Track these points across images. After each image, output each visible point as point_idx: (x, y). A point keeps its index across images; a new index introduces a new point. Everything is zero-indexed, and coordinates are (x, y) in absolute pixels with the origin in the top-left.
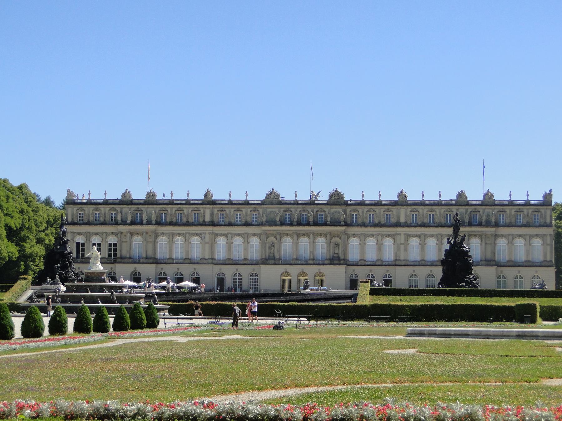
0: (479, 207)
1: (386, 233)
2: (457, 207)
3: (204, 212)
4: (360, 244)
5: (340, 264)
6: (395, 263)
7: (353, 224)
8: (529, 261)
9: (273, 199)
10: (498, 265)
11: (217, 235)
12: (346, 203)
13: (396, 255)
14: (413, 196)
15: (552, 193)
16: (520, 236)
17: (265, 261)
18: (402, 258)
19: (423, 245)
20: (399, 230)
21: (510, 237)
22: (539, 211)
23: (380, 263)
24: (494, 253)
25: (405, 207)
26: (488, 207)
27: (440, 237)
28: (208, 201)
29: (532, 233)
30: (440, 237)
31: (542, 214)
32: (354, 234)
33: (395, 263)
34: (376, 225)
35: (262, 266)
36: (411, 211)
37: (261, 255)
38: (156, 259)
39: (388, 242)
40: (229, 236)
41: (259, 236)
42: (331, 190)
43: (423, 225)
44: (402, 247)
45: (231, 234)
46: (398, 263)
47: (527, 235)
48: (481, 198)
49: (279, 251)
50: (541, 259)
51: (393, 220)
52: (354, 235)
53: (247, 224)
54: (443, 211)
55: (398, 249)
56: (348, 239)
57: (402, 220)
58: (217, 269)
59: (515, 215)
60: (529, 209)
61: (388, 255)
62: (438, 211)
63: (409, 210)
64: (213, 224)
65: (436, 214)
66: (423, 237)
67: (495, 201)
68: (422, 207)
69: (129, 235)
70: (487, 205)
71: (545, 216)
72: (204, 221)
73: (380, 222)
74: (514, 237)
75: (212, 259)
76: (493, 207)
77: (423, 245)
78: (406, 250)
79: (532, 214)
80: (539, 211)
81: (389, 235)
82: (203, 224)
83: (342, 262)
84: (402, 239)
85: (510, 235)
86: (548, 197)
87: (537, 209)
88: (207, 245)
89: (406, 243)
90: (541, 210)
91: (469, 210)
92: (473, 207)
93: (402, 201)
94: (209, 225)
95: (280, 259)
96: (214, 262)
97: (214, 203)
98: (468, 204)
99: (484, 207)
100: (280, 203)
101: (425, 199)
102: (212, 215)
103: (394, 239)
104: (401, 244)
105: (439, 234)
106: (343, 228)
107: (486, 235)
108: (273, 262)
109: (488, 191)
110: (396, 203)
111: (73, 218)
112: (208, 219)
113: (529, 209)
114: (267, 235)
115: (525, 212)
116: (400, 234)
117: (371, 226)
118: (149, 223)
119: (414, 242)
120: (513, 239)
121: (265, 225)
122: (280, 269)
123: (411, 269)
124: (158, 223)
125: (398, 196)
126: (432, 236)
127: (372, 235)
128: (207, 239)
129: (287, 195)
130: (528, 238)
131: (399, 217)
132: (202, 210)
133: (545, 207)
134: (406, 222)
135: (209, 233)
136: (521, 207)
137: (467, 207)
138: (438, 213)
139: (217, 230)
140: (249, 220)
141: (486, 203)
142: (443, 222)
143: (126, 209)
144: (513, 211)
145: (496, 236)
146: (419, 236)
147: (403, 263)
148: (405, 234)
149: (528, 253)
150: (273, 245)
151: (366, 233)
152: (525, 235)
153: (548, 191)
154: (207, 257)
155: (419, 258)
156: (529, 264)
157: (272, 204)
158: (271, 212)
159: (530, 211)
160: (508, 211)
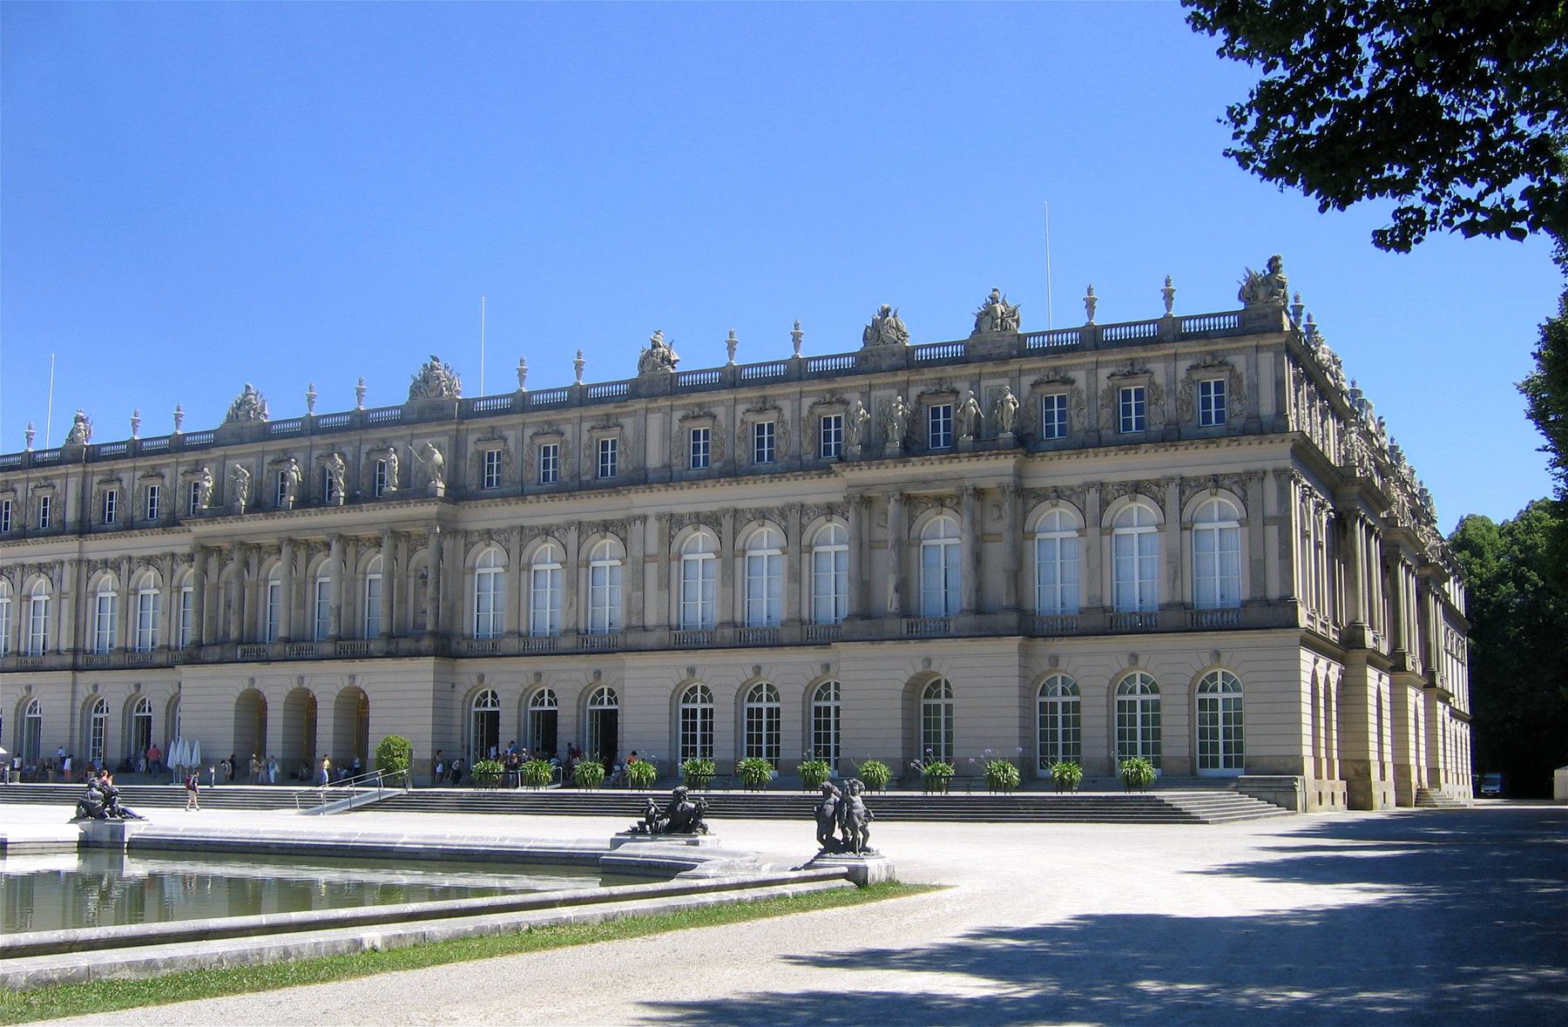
0: (950, 371)
1: (597, 518)
2: (861, 381)
4: (507, 567)
7: (487, 491)
8: (1184, 606)
10: (1030, 626)
11: (92, 566)
12: (468, 411)
13: (635, 607)
14: (695, 355)
15: (1283, 275)
16: (1136, 489)
18: (651, 620)
19: (732, 558)
21: (1092, 497)
22: (1223, 364)
24: (1017, 575)
25: (663, 402)
26: (989, 368)
27: (794, 518)
29: (1189, 472)
30: (794, 518)
31: (1235, 377)
32: (489, 532)
35: (186, 671)
36: (684, 419)
39: (606, 554)
40: (125, 566)
44: (652, 570)
45: (130, 559)
47: (1170, 480)
48: (965, 331)
50: (1240, 589)
52: (488, 535)
56: (467, 552)
57: (654, 460)
59: (1112, 390)
60: (1176, 356)
61: (609, 606)
62: (786, 406)
64: (83, 529)
65: (781, 421)
66: (727, 523)
67: (1022, 338)
68: (725, 395)
70: (986, 359)
71: (1255, 387)
72: (63, 522)
74: (1106, 493)
76: (1013, 366)
77: (732, 558)
79: (1189, 381)
80: (1223, 364)
81: (606, 527)
82: (59, 531)
83: (426, 643)
85: (1088, 486)
87: (1213, 354)
89: (670, 556)
90: (1229, 359)
91: (914, 392)
92: (930, 374)
93: (657, 382)
94: (72, 533)
96: (80, 661)
98: (909, 361)
99: (971, 369)
103: (624, 541)
105: (790, 507)
107: (979, 493)
108: (216, 652)
109: (994, 300)
110: (635, 390)
112: (71, 515)
113: (1176, 356)
115: (1159, 372)
116: (644, 518)
119: (700, 545)
120: (1104, 504)
123: (746, 659)
126: (763, 515)
127: (547, 532)
130: (1172, 492)
132: (58, 482)
133: (1250, 342)
134: (668, 466)
135: (71, 562)
136: (1139, 353)
137: (902, 377)
138: (787, 415)
139: (99, 547)
141: (982, 351)
144: (1104, 373)
145: (1024, 495)
146: (712, 520)
148: (659, 517)
149: (1176, 565)
151: (527, 522)
152: (1157, 483)
153: (1260, 268)
154: (64, 646)
155: (716, 615)
156: (1186, 618)
159: (1183, 365)
160: (1080, 377)
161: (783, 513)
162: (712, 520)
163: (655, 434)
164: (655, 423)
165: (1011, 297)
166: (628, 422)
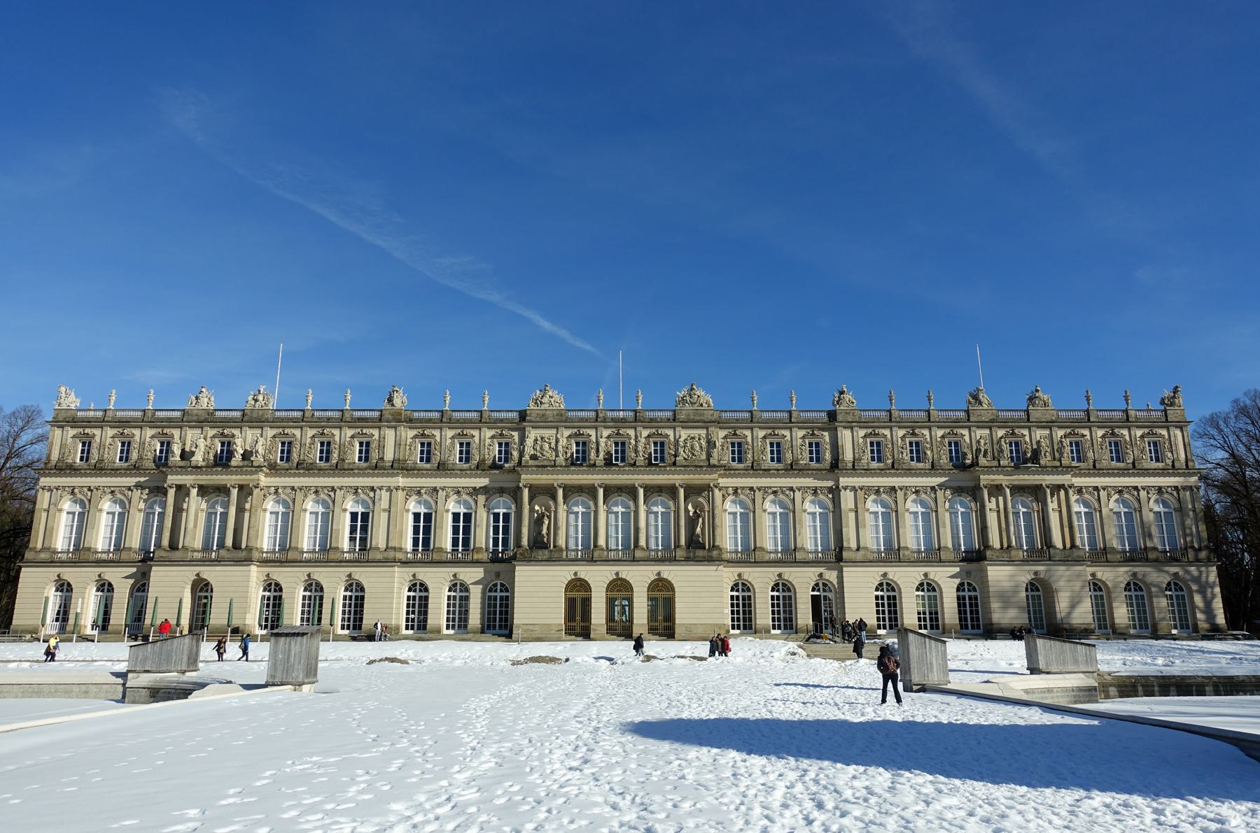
3: (382, 440)
20: (844, 481)
57: (848, 455)
64: (400, 466)
66: (900, 494)
82: (378, 468)
83: (715, 553)
96: (399, 556)
102: (397, 445)
104: (851, 510)
111: (62, 454)
112: (389, 455)
116: (845, 488)
122: (564, 574)
143: (191, 434)
147: (859, 556)
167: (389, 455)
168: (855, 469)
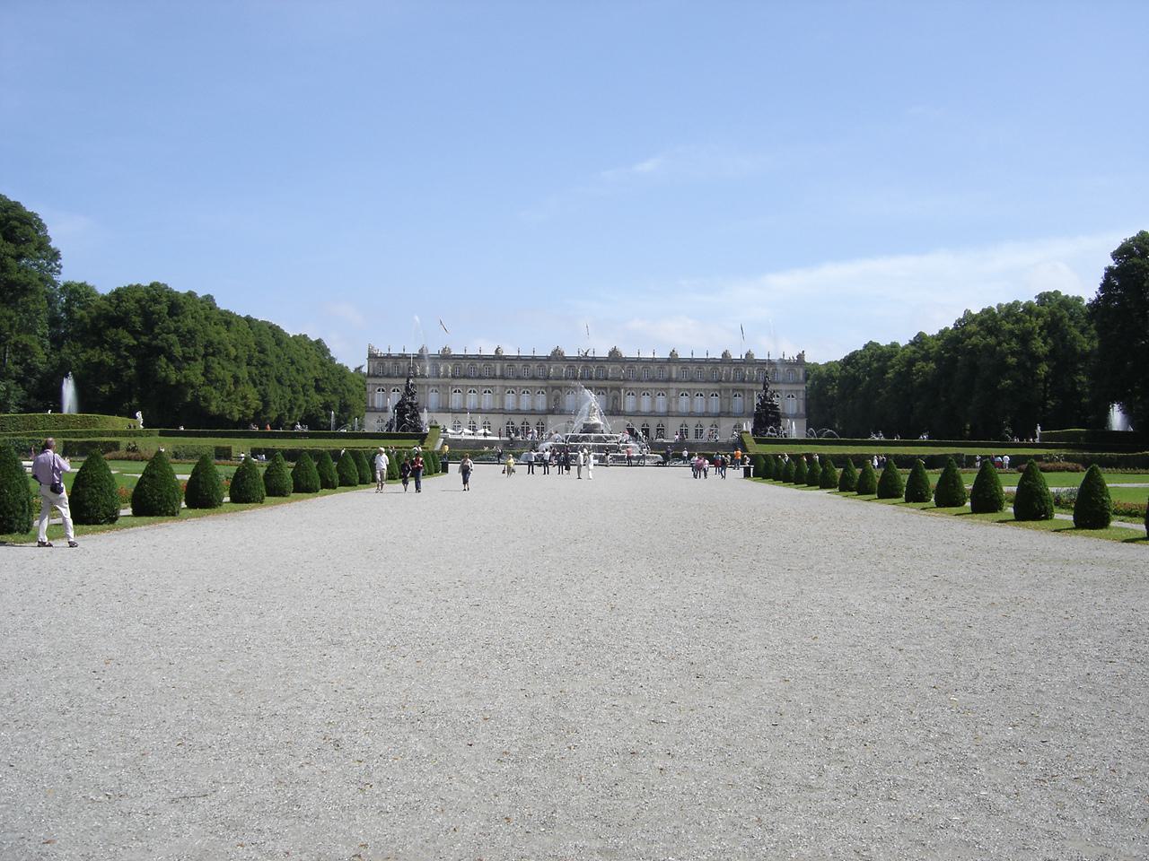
5: (619, 415)
6: (668, 414)
9: (557, 356)
11: (506, 387)
13: (668, 405)
14: (683, 354)
17: (550, 412)
18: (674, 410)
20: (671, 385)
23: (653, 414)
28: (498, 357)
33: (668, 414)
34: (651, 380)
35: (549, 416)
37: (548, 405)
38: (448, 408)
41: (546, 388)
42: (610, 349)
43: (692, 381)
46: (670, 414)
49: (563, 403)
50: (795, 411)
51: (666, 376)
53: (534, 378)
54: (710, 368)
55: (670, 401)
57: (674, 376)
58: (507, 418)
61: (661, 404)
63: (680, 367)
64: (503, 377)
69: (426, 387)
70: (748, 363)
73: (654, 377)
75: (503, 409)
78: (677, 402)
82: (494, 377)
84: (673, 393)
86: (801, 356)
88: (498, 397)
89: (677, 397)
93: (673, 360)
95: (564, 411)
97: (505, 358)
100: (565, 359)
101: (694, 357)
102: (502, 369)
106: (622, 383)
112: (498, 373)
114: (554, 388)
117: (646, 381)
118: (446, 376)
121: (551, 379)
124: (453, 377)
125: (671, 354)
128: (498, 391)
129: (570, 352)
131: (670, 373)
132: (493, 365)
134: (677, 378)
139: (508, 383)
140: (537, 374)
142: (710, 379)
147: (674, 414)
150: (557, 398)
153: (801, 352)
157: (557, 360)
158: (556, 368)
161: (705, 389)
162: (689, 390)
163: (674, 371)
164: (674, 368)
165: (752, 352)
166: (667, 368)
167: (498, 373)
168: (676, 382)
